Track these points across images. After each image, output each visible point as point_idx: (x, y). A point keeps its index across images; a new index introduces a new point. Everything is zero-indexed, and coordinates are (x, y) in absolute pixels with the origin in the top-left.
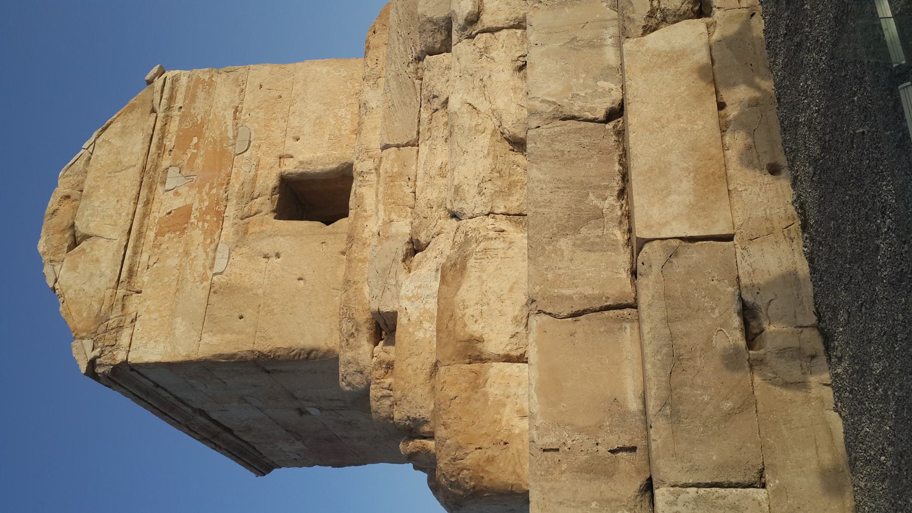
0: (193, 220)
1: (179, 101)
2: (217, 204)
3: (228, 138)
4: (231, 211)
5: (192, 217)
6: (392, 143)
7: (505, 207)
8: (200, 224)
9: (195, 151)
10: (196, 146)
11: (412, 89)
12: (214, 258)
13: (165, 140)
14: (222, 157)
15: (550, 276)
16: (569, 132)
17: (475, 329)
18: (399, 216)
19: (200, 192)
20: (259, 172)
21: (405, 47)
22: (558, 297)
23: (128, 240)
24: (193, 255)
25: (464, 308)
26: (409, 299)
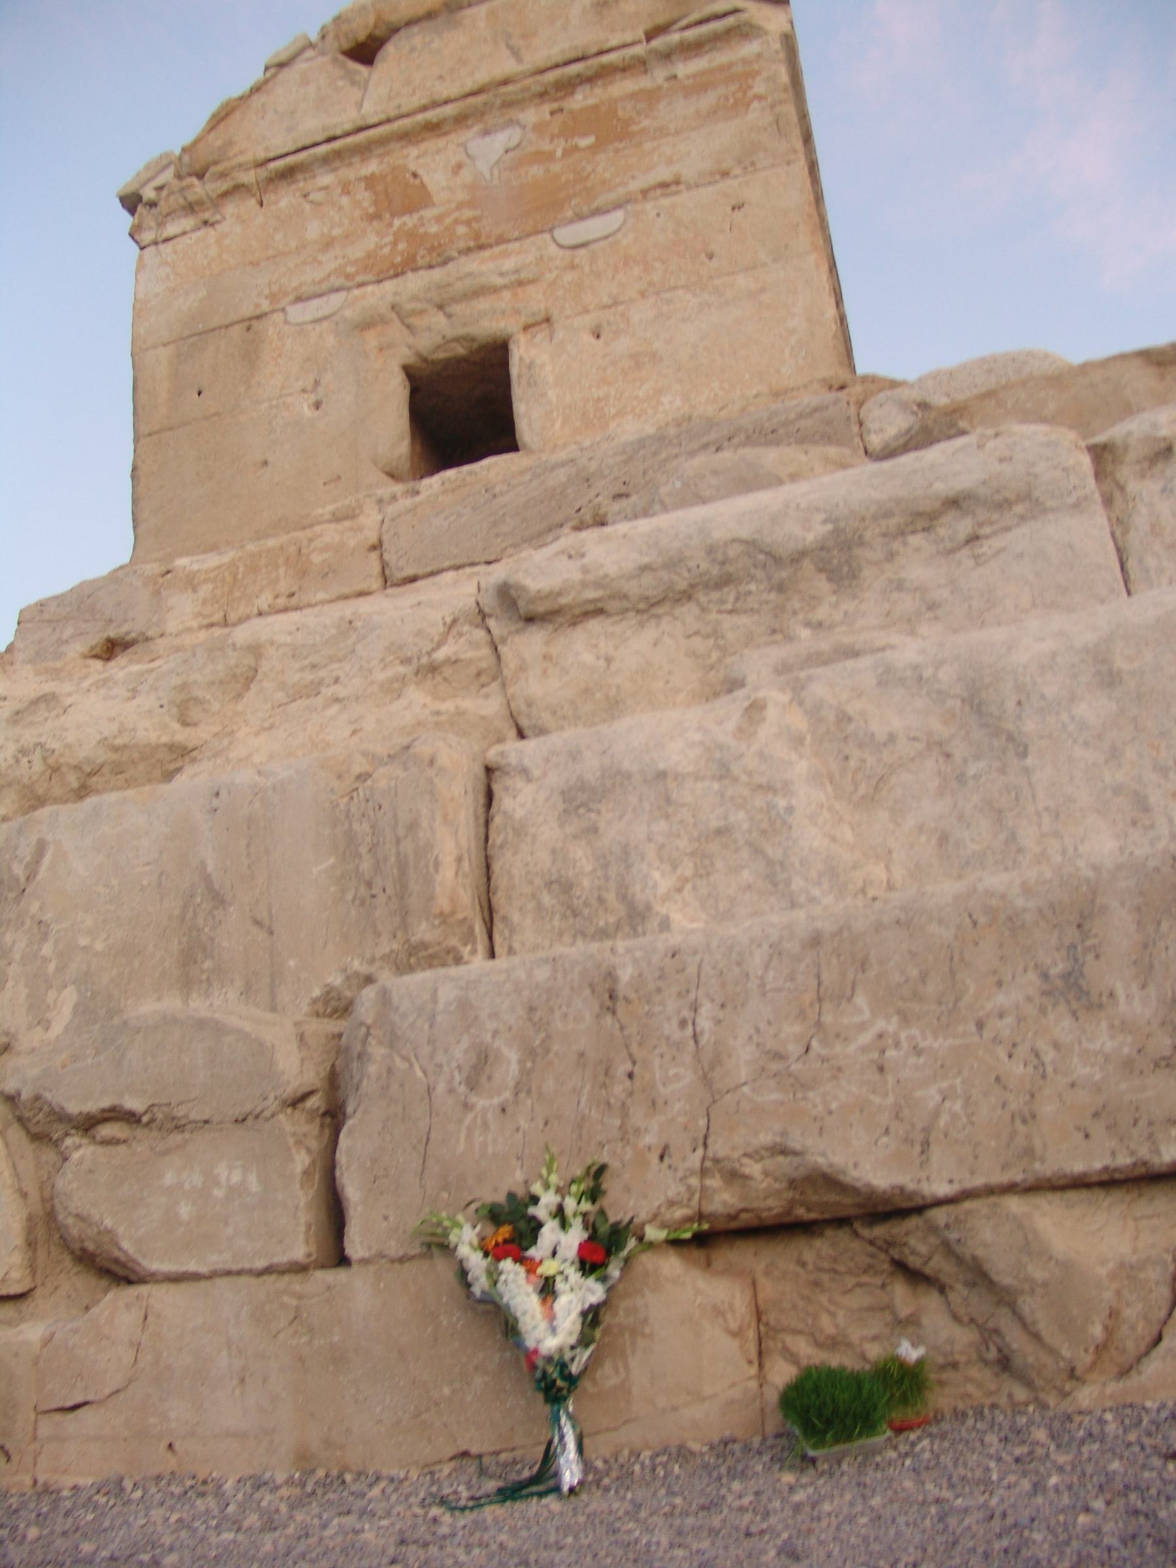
0: (397, 223)
1: (685, 69)
2: (432, 249)
5: (406, 218)
9: (559, 153)
12: (320, 295)
13: (587, 87)
14: (543, 208)
19: (460, 206)
20: (507, 295)
23: (348, 134)
24: (322, 258)
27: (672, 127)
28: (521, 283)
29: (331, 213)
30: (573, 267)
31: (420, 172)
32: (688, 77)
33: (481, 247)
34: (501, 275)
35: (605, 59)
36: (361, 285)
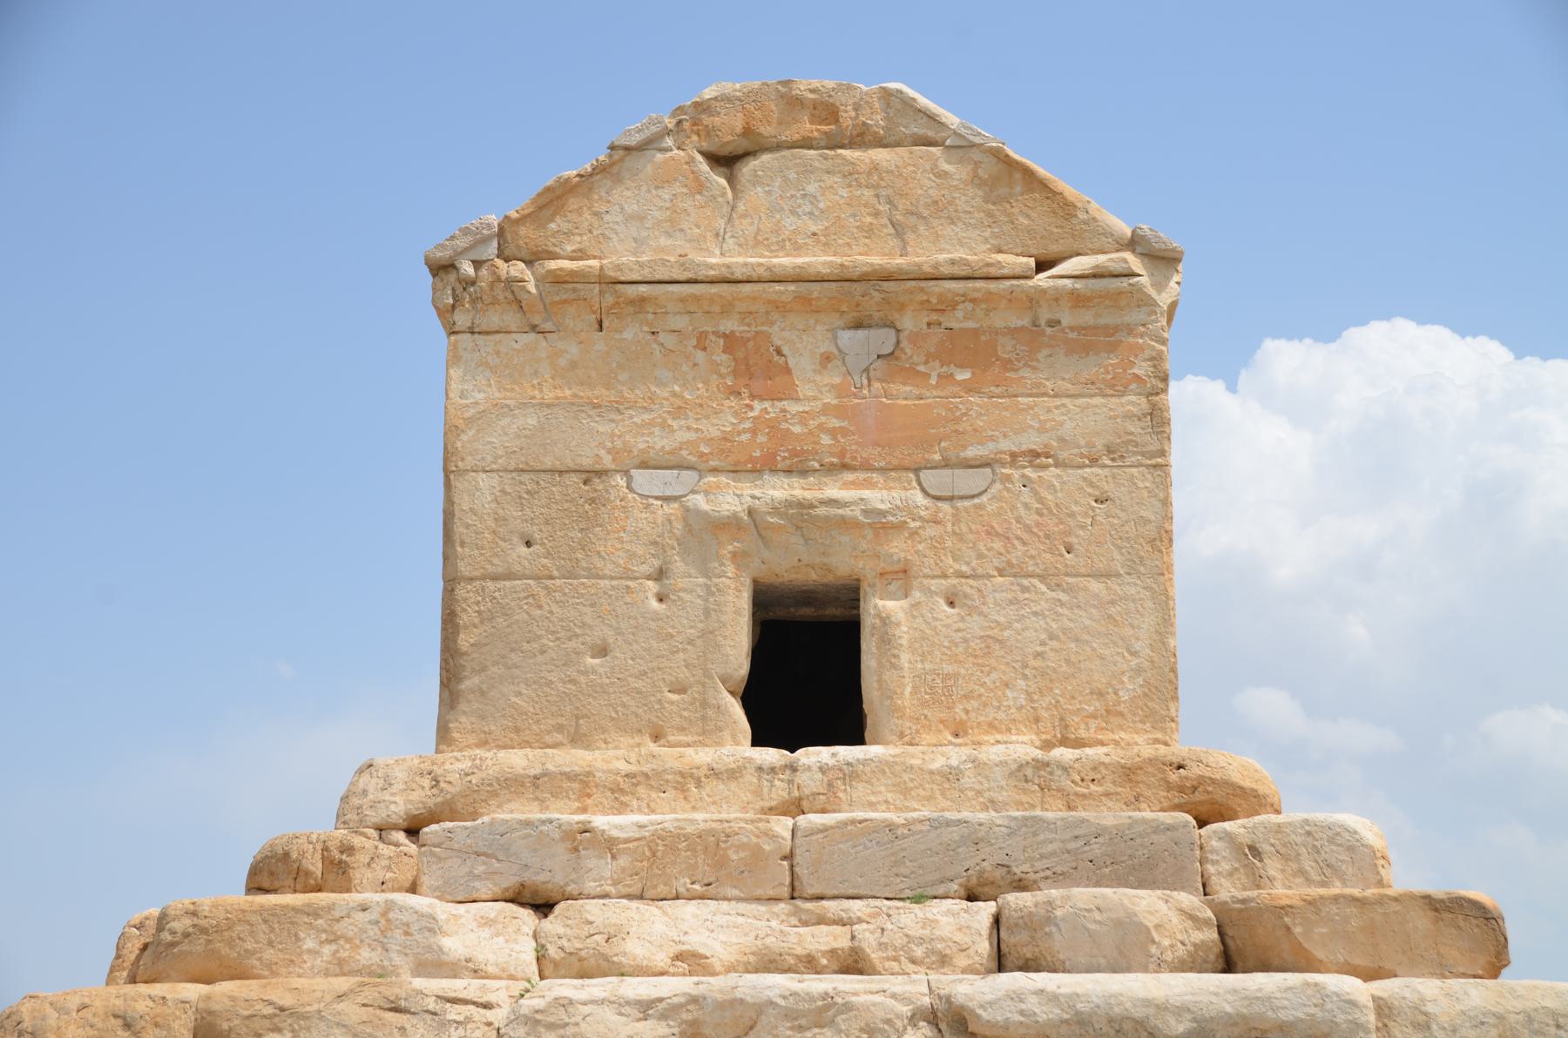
0: (757, 405)
2: (794, 453)
3: (964, 447)
4: (778, 489)
5: (767, 404)
6: (798, 841)
8: (748, 425)
11: (937, 876)
13: (969, 306)
18: (623, 870)
19: (826, 410)
21: (1054, 853)
24: (675, 424)
28: (885, 526)
29: (685, 368)
31: (785, 350)
32: (1072, 329)
33: (845, 467)
36: (715, 471)
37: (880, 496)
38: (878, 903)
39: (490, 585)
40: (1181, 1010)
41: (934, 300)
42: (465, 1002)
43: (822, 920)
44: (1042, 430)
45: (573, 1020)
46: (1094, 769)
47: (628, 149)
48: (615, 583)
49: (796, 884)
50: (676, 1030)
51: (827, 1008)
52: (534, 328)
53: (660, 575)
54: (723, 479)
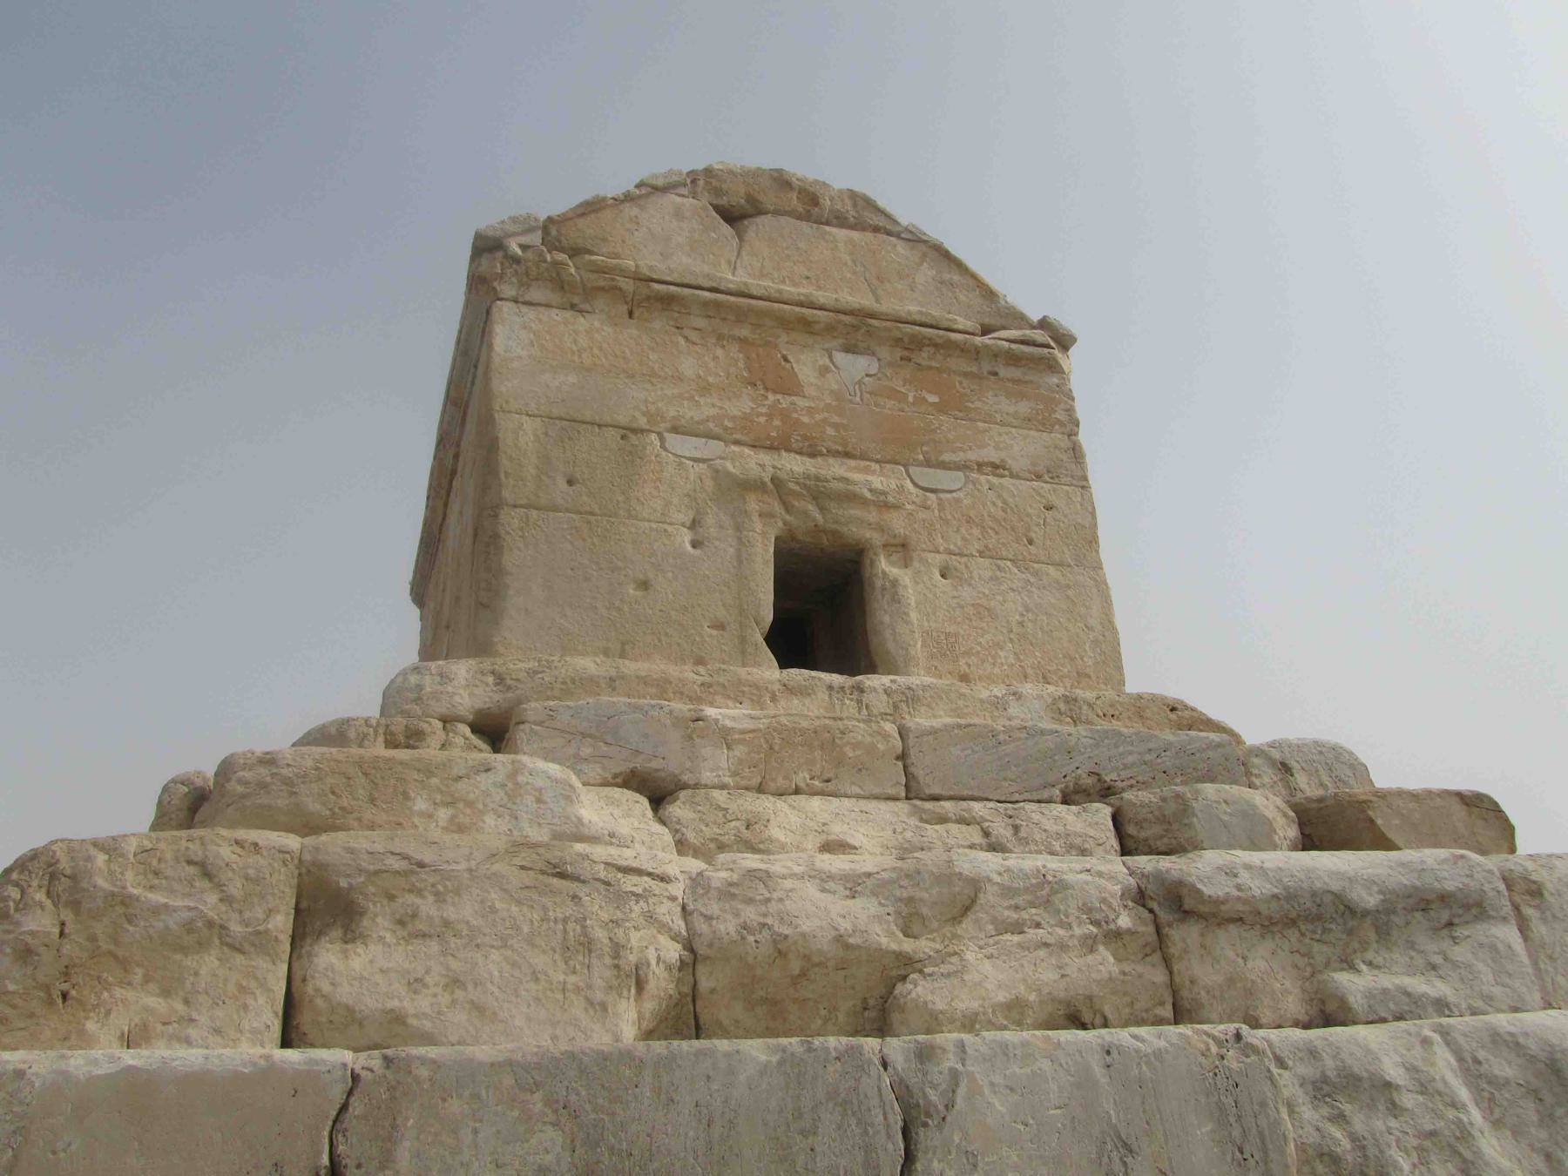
0: (771, 397)
2: (805, 438)
3: (941, 453)
4: (794, 464)
5: (779, 397)
6: (911, 742)
7: (713, 991)
8: (764, 410)
9: (911, 399)
10: (920, 401)
13: (932, 350)
15: (455, 1106)
16: (868, 1149)
17: (379, 922)
18: (740, 761)
19: (828, 408)
22: (394, 1127)
23: (731, 294)
24: (702, 401)
25: (437, 894)
26: (513, 775)
27: (998, 417)
30: (927, 508)
33: (847, 455)
34: (871, 490)
35: (954, 336)
36: (737, 443)
37: (878, 480)
38: (991, 804)
39: (534, 513)
40: (1370, 883)
41: (906, 340)
42: (639, 872)
43: (943, 820)
44: (997, 448)
45: (775, 895)
46: (1112, 706)
47: (656, 189)
48: (654, 526)
49: (913, 784)
50: (891, 909)
51: (1040, 886)
52: (573, 307)
53: (694, 525)
54: (746, 450)
